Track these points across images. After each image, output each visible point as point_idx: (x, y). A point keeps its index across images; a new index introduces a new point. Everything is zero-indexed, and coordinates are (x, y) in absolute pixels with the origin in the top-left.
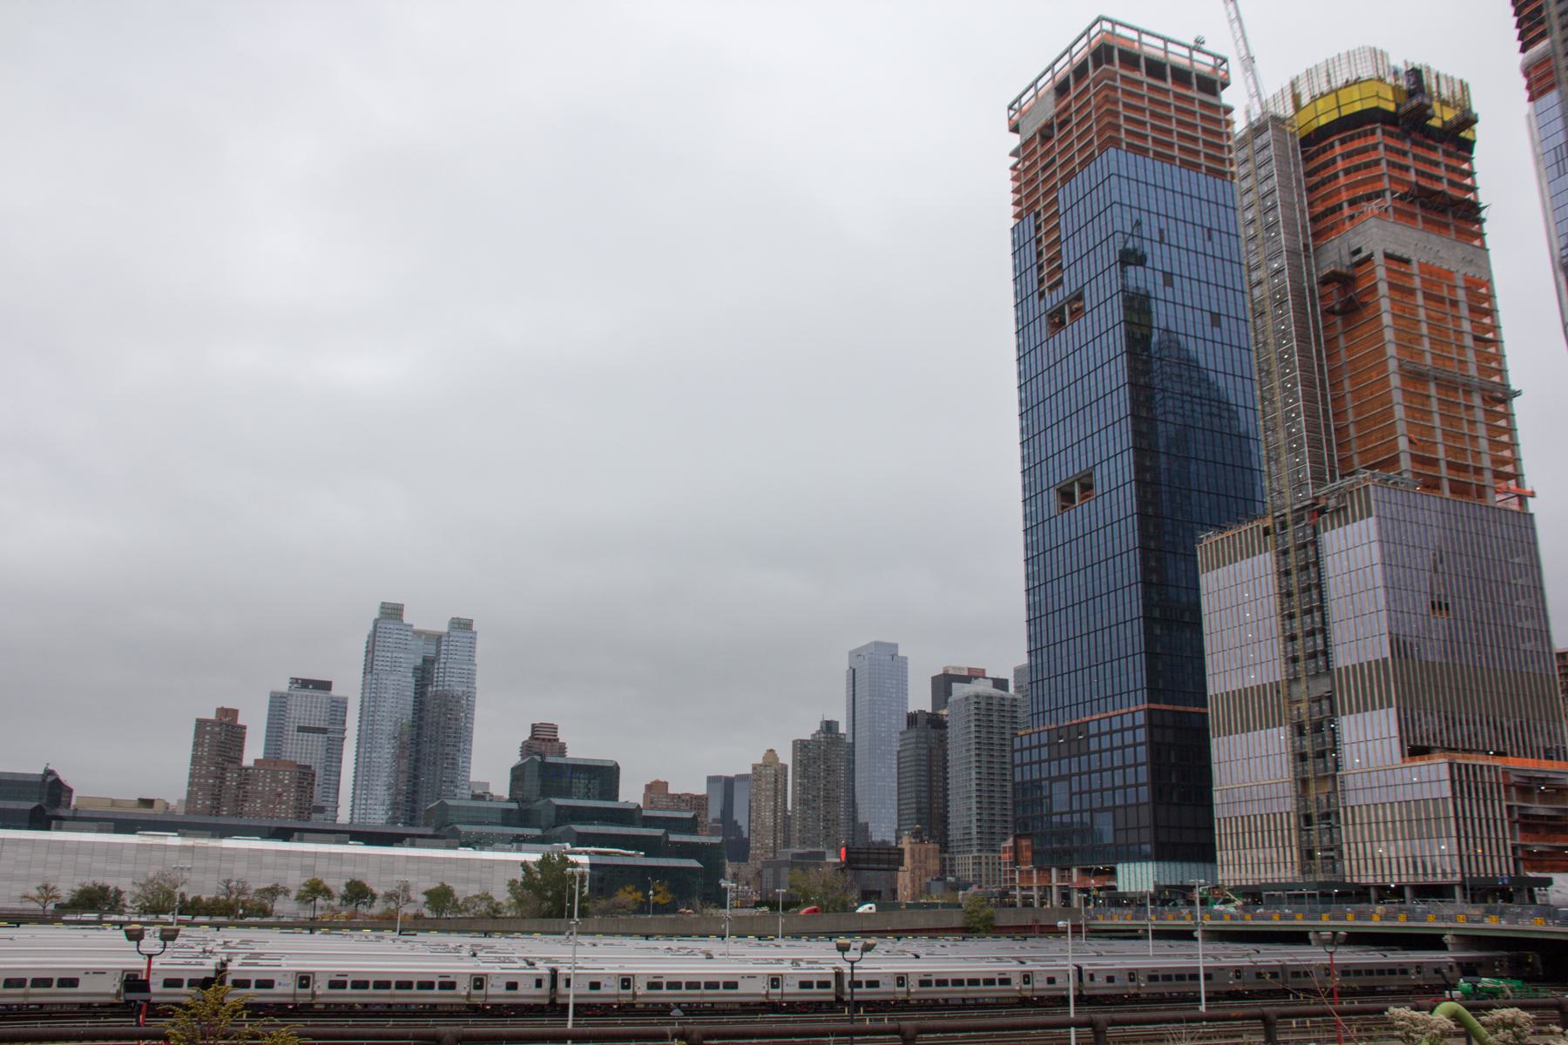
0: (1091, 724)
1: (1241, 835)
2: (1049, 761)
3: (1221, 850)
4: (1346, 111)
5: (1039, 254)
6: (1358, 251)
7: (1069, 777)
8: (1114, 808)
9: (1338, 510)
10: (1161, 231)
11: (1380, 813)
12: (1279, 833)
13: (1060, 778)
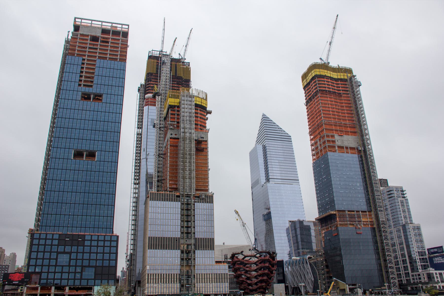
0: (86, 236)
2: (58, 245)
3: (148, 283)
4: (203, 104)
5: (82, 72)
8: (96, 267)
9: (203, 199)
12: (173, 280)
13: (64, 253)
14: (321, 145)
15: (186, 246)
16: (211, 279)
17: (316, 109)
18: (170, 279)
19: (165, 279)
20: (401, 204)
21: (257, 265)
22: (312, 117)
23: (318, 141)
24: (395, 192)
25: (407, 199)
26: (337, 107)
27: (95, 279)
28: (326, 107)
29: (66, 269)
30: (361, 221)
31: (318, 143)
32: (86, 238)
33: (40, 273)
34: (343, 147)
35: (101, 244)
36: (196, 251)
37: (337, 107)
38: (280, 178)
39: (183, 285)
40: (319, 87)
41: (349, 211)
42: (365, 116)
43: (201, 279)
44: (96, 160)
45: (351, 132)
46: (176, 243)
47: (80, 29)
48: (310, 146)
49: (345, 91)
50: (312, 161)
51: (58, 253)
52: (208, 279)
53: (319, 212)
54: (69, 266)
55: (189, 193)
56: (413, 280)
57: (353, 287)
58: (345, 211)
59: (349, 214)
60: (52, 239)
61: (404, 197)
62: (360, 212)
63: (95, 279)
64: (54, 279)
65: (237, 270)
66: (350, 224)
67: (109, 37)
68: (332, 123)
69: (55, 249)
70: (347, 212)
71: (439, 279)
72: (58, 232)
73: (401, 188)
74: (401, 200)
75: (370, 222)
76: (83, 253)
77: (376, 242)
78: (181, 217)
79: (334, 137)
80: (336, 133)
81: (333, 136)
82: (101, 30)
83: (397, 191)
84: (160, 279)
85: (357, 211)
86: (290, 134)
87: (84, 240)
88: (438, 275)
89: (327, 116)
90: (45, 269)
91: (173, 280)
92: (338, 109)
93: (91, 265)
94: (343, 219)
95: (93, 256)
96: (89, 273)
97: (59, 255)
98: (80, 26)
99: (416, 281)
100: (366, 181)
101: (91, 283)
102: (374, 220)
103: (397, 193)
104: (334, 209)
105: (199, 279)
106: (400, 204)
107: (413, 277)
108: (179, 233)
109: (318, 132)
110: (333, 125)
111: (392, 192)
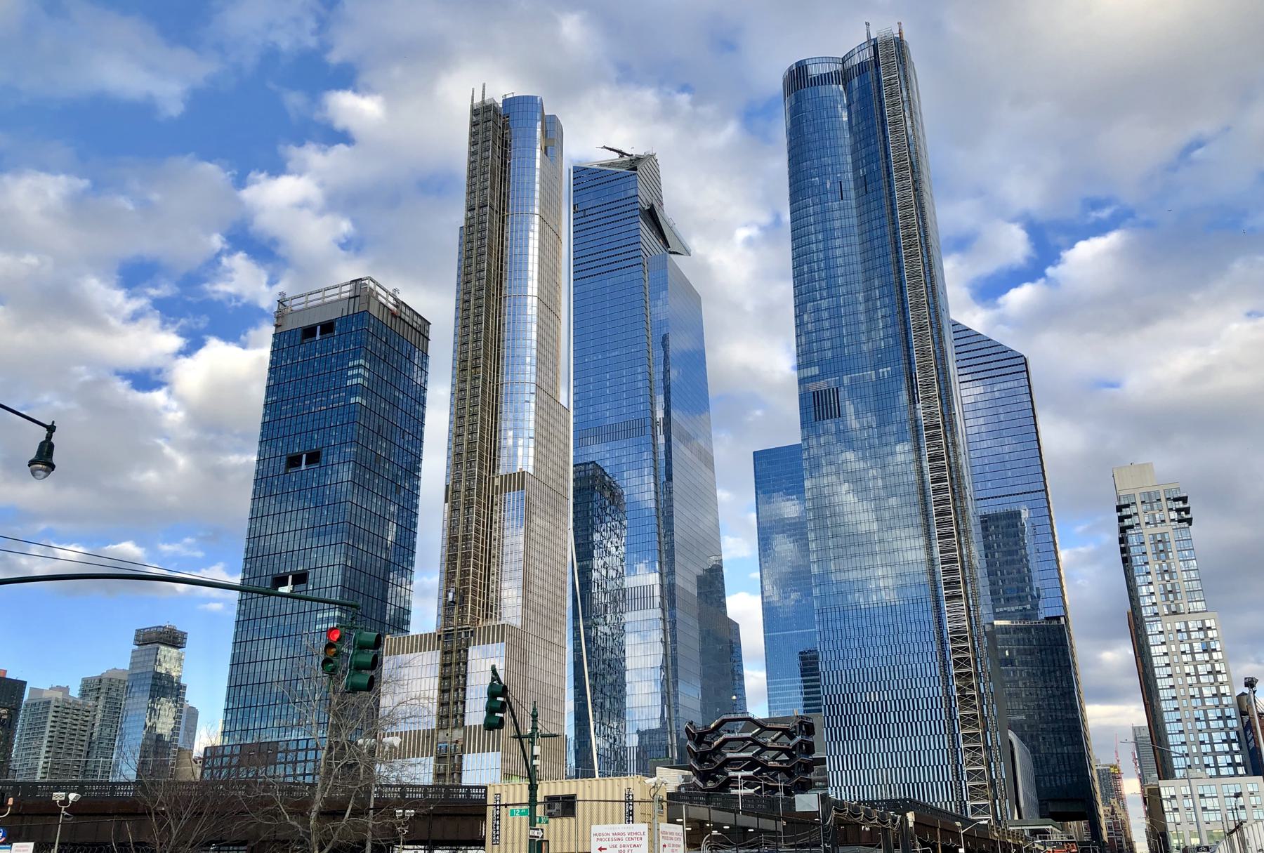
2: (238, 766)
10: (379, 426)
20: (1157, 547)
74: (1154, 536)
83: (1151, 503)
106: (1148, 548)
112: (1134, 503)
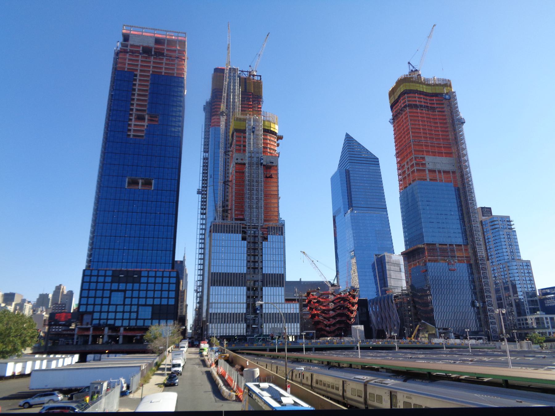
0: (142, 272)
1: (220, 319)
2: (112, 282)
6: (273, 163)
7: (125, 291)
8: (153, 306)
11: (277, 315)
12: (238, 319)
13: (118, 290)
14: (408, 168)
15: (252, 283)
16: (280, 319)
17: (405, 126)
18: (235, 319)
19: (229, 319)
21: (335, 304)
22: (399, 136)
23: (406, 164)
24: (501, 223)
25: (515, 231)
26: (429, 124)
27: (152, 319)
28: (416, 125)
29: (120, 309)
30: (455, 257)
31: (406, 166)
32: (143, 274)
33: (92, 313)
34: (435, 170)
35: (159, 280)
36: (264, 288)
37: (429, 124)
38: (365, 206)
39: (249, 325)
40: (409, 101)
41: (440, 244)
42: (463, 133)
43: (269, 319)
44: (153, 189)
45: (445, 153)
46: (242, 279)
47: (130, 39)
48: (397, 170)
49: (439, 104)
50: (399, 187)
51: (112, 291)
52: (277, 319)
53: (406, 245)
54: (124, 305)
55: (256, 225)
56: (519, 325)
57: (444, 331)
58: (435, 244)
59: (440, 248)
60: (105, 276)
61: (512, 229)
62: (454, 245)
63: (152, 319)
64: (107, 319)
65: (313, 309)
66: (442, 260)
67: (163, 47)
68: (422, 142)
69: (107, 286)
70: (437, 245)
71: (550, 325)
72: (112, 267)
73: (509, 217)
74: (507, 232)
75: (466, 257)
76: (139, 290)
77: (473, 281)
78: (247, 251)
79: (425, 159)
80: (427, 155)
81: (423, 158)
82: (154, 39)
84: (223, 319)
85: (450, 245)
86: (378, 157)
87: (140, 277)
88: (549, 320)
89: (416, 135)
90: (98, 308)
91: (238, 319)
92: (431, 126)
93: (148, 303)
94: (434, 254)
95: (150, 294)
96: (146, 313)
97: (113, 293)
98: (130, 35)
99: (522, 326)
100: (462, 210)
101: (148, 323)
102: (471, 255)
103: (503, 223)
104: (422, 241)
105: (267, 318)
107: (519, 322)
108: (245, 268)
109: (405, 153)
110: (424, 145)
111: (495, 223)
112: (498, 221)
